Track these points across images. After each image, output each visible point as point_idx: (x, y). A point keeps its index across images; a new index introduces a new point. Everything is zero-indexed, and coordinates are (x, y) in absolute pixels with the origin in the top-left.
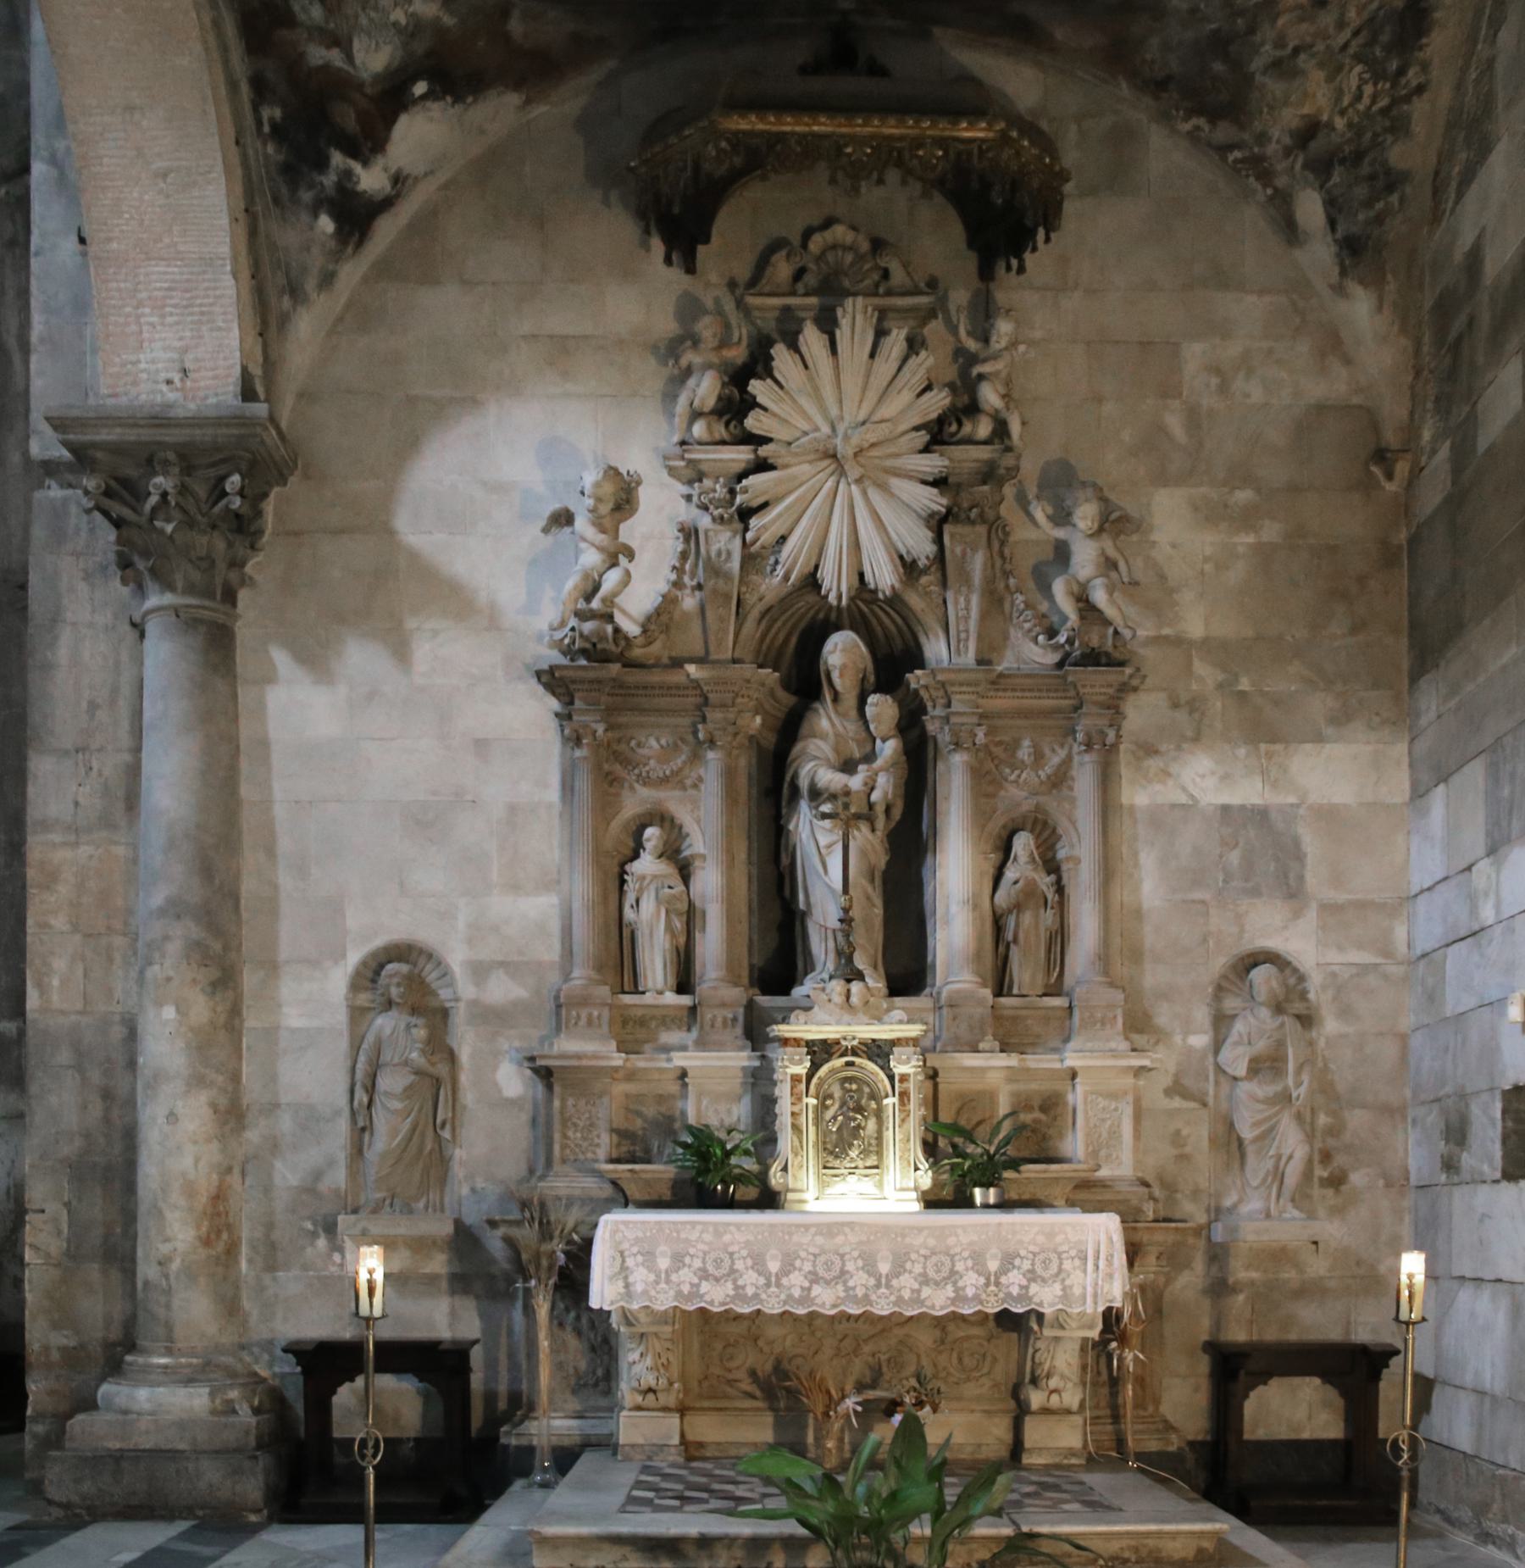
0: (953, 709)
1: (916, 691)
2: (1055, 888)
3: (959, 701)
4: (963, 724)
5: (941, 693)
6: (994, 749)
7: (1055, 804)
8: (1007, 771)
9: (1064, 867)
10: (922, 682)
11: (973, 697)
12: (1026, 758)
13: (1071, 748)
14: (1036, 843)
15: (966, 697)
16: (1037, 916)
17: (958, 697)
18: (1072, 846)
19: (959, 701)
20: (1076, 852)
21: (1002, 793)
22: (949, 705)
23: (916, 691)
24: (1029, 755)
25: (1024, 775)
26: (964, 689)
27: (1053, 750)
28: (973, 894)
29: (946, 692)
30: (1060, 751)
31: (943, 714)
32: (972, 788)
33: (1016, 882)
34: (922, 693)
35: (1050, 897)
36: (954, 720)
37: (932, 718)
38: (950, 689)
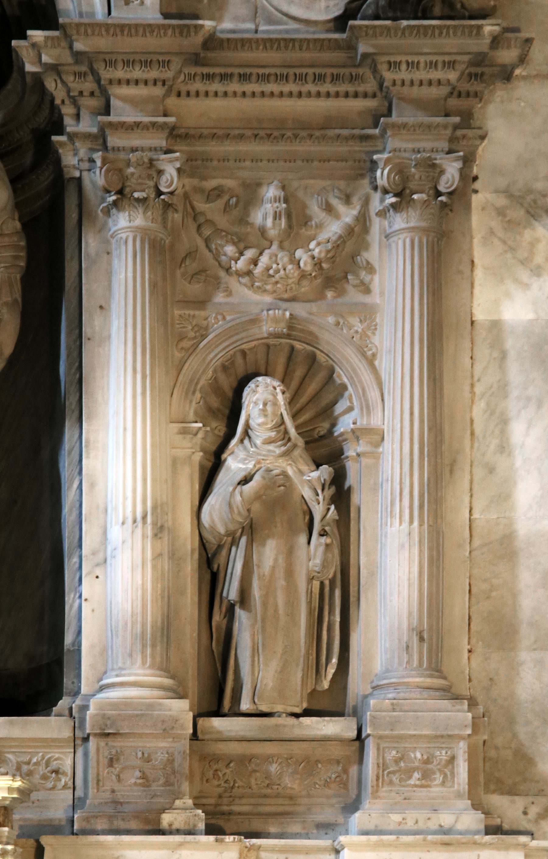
0: (112, 118)
1: (38, 79)
2: (330, 492)
3: (124, 99)
4: (134, 150)
5: (89, 85)
6: (201, 206)
7: (331, 320)
8: (230, 250)
9: (350, 451)
10: (45, 58)
11: (158, 91)
12: (269, 222)
13: (366, 202)
14: (291, 402)
15: (141, 91)
16: (290, 552)
17: (124, 91)
18: (367, 409)
19: (124, 99)
20: (376, 421)
21: (220, 298)
22: (107, 111)
23: (38, 79)
24: (276, 216)
25: (264, 260)
26: (137, 73)
27: (329, 209)
28: (154, 508)
29: (98, 81)
30: (341, 208)
31: (95, 130)
32: (154, 286)
33: (246, 480)
34: (50, 84)
35: (318, 511)
36: (113, 140)
37: (72, 137)
38: (106, 74)
